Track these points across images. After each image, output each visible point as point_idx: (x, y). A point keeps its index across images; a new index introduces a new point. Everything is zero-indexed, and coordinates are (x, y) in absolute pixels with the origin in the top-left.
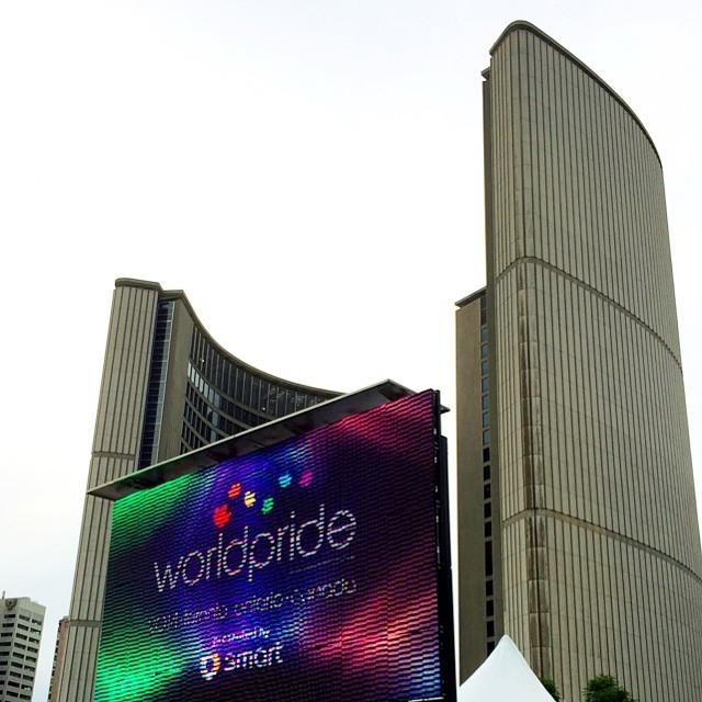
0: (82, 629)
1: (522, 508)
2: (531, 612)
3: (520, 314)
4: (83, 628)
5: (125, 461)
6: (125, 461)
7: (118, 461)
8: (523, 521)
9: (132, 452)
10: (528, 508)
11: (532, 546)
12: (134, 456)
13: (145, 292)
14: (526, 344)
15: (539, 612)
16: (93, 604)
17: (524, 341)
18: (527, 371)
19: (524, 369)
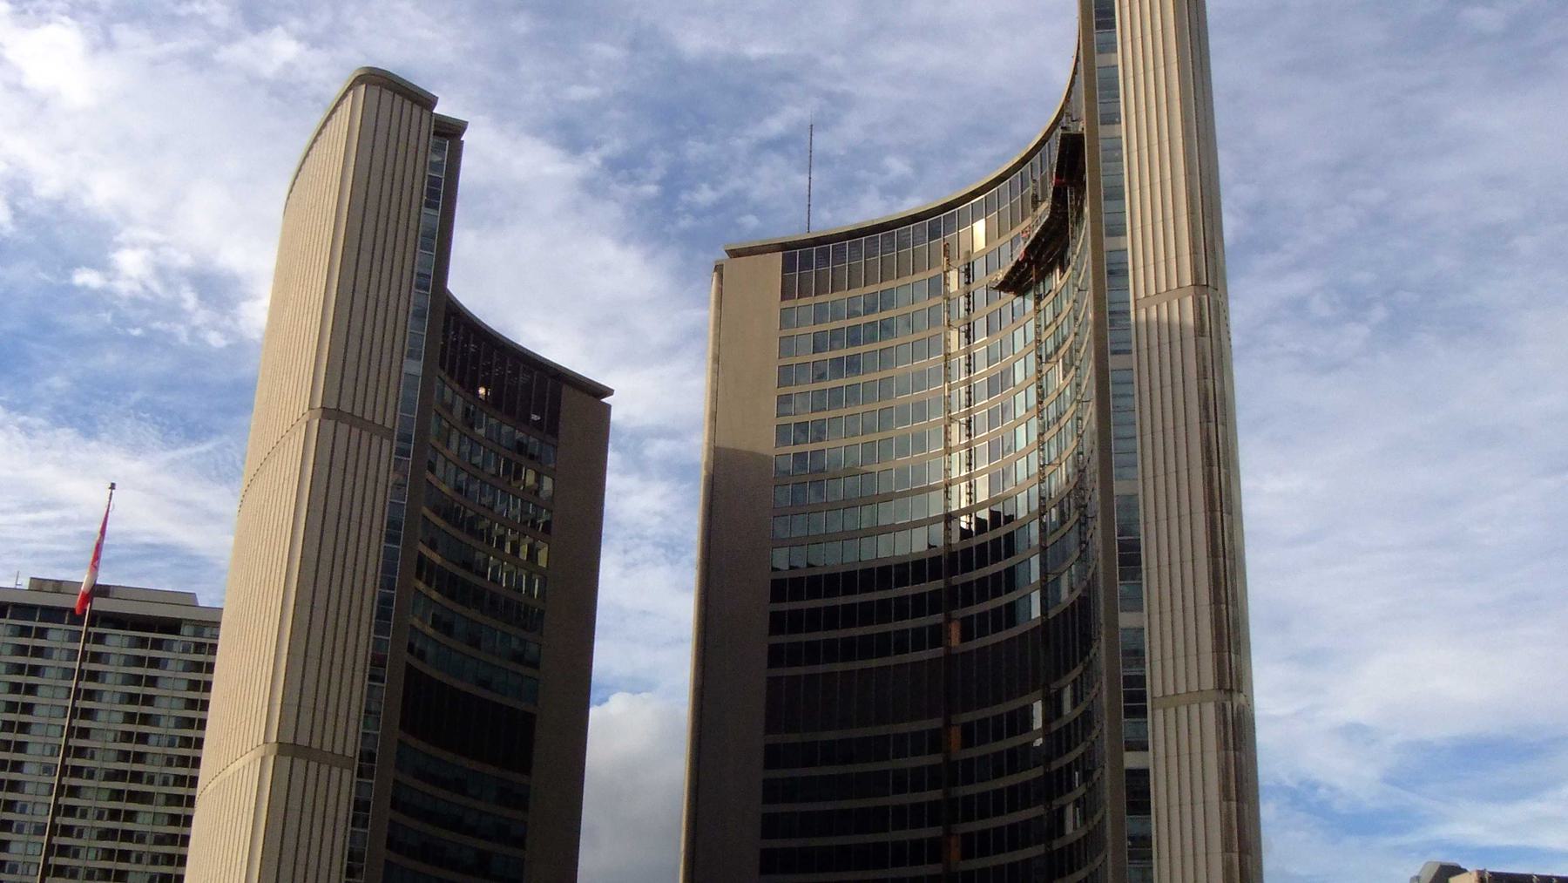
0: (300, 764)
1: (1209, 682)
2: (1227, 848)
3: (1202, 375)
4: (304, 762)
5: (376, 440)
6: (376, 440)
7: (365, 435)
8: (1210, 710)
9: (388, 425)
10: (1220, 689)
11: (1226, 749)
12: (392, 430)
13: (416, 110)
14: (1212, 425)
15: (1240, 853)
16: (319, 717)
17: (1208, 422)
18: (1215, 469)
19: (1210, 465)
